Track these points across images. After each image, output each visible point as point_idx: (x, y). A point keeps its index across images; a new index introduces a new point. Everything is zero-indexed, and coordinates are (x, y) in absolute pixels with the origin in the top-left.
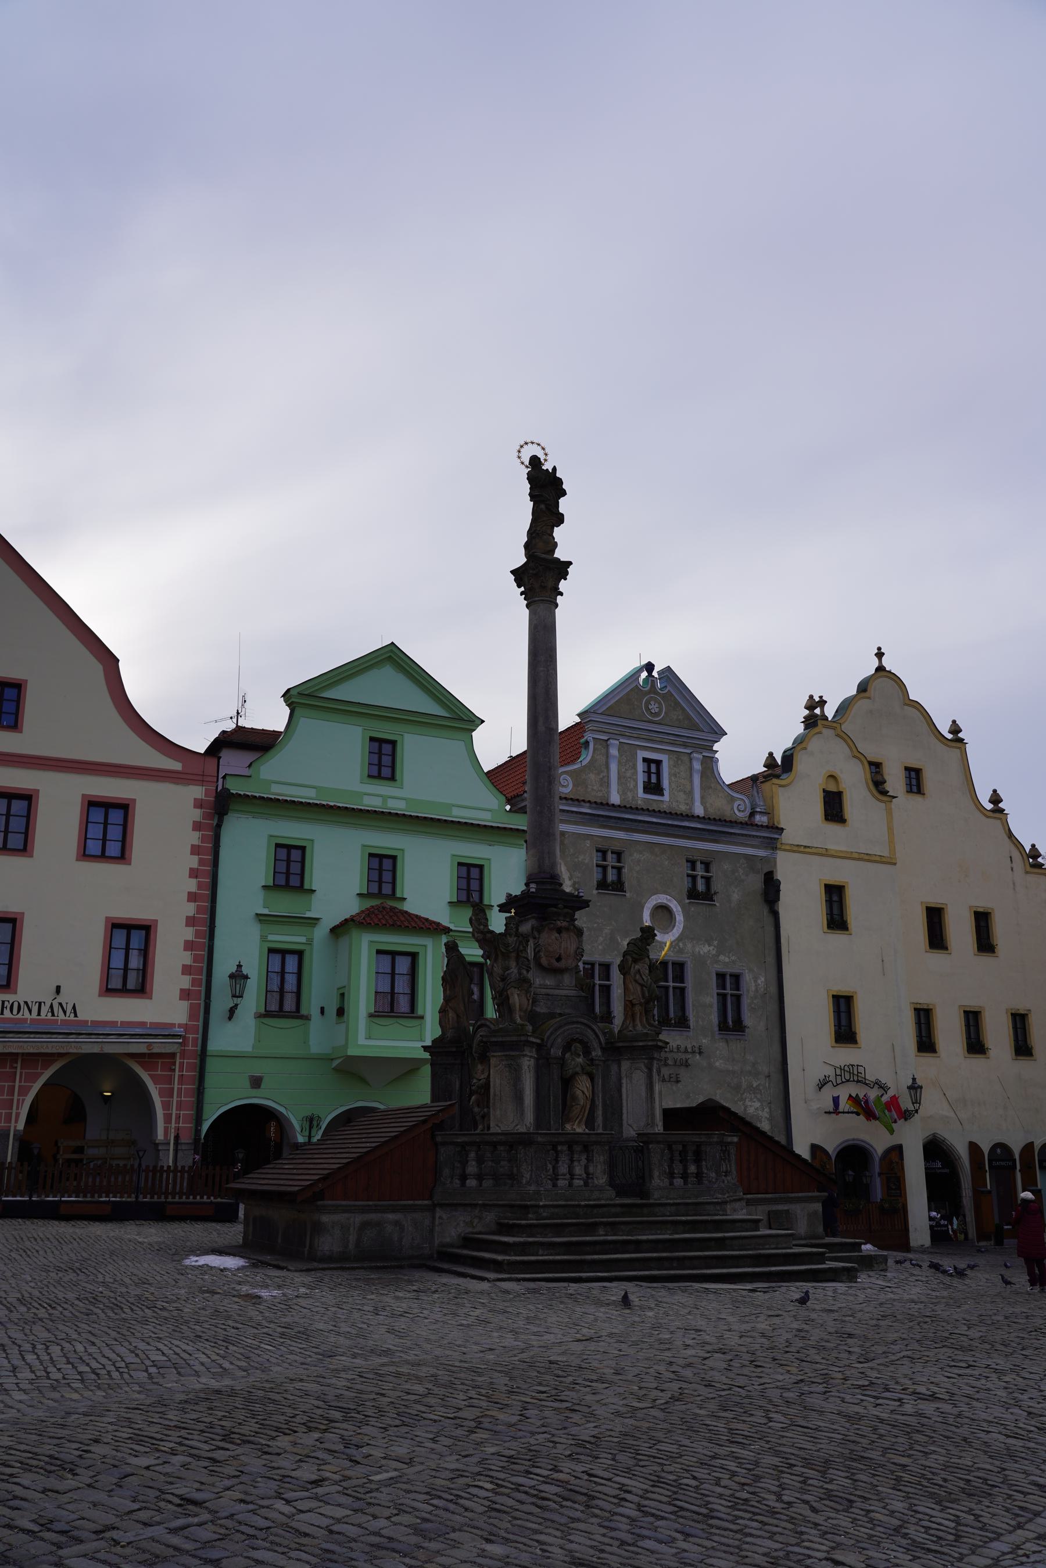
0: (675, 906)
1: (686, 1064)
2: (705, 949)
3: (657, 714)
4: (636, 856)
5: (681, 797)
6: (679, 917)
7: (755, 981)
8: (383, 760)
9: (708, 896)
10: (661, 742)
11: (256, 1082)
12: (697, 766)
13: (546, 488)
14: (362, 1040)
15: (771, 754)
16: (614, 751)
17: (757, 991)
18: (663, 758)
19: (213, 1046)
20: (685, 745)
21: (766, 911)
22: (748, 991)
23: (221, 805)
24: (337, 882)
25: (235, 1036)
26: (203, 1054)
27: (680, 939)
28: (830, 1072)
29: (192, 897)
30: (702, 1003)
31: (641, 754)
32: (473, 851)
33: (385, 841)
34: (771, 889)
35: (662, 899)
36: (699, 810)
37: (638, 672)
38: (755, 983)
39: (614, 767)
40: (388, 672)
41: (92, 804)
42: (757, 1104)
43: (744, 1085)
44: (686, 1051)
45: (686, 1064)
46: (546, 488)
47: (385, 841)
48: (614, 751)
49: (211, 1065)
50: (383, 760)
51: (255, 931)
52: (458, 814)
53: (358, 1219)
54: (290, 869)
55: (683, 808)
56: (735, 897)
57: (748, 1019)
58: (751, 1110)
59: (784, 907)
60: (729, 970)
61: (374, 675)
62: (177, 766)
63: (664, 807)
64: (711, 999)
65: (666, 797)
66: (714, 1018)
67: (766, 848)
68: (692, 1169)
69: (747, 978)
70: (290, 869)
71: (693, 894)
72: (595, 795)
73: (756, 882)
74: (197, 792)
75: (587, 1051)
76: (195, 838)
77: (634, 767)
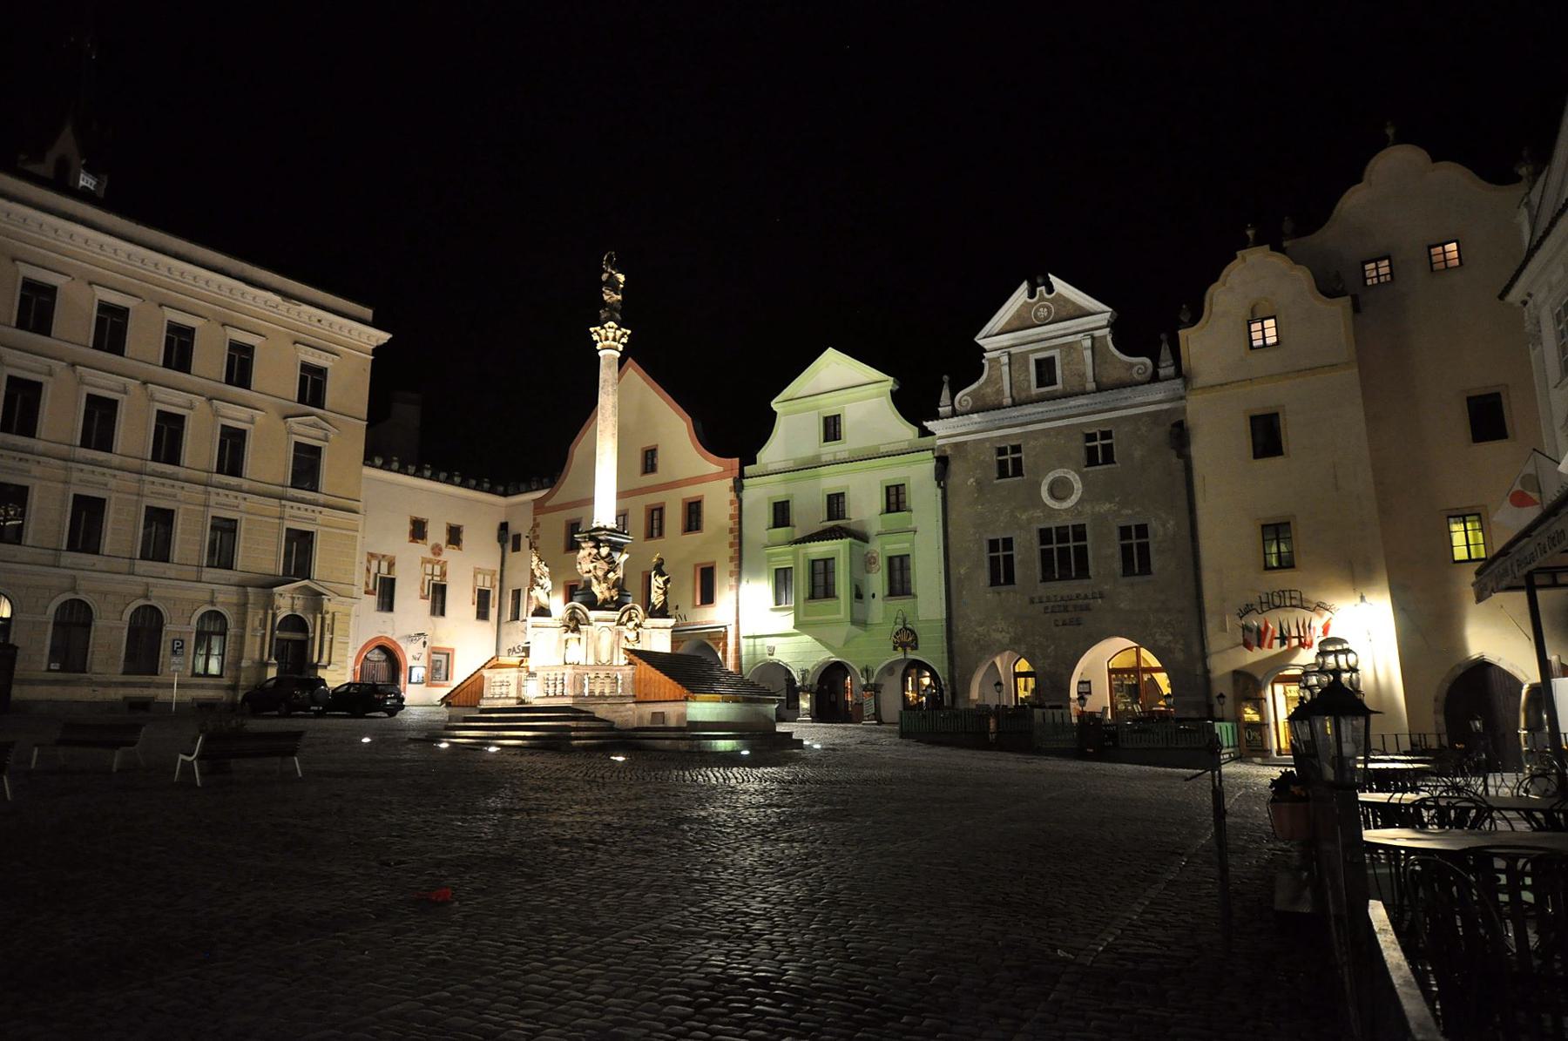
1: (1087, 608)
2: (1107, 506)
6: (1078, 486)
9: (1108, 457)
18: (1056, 353)
27: (1081, 501)
28: (1253, 598)
30: (1104, 553)
31: (1032, 358)
34: (1179, 435)
35: (1059, 473)
38: (1162, 528)
45: (1087, 608)
52: (883, 449)
56: (1138, 453)
57: (1156, 562)
58: (1162, 644)
59: (1200, 451)
60: (1133, 523)
64: (1114, 549)
65: (1059, 386)
66: (1117, 565)
69: (1154, 526)
71: (1092, 459)
74: (729, 482)
77: (1027, 370)
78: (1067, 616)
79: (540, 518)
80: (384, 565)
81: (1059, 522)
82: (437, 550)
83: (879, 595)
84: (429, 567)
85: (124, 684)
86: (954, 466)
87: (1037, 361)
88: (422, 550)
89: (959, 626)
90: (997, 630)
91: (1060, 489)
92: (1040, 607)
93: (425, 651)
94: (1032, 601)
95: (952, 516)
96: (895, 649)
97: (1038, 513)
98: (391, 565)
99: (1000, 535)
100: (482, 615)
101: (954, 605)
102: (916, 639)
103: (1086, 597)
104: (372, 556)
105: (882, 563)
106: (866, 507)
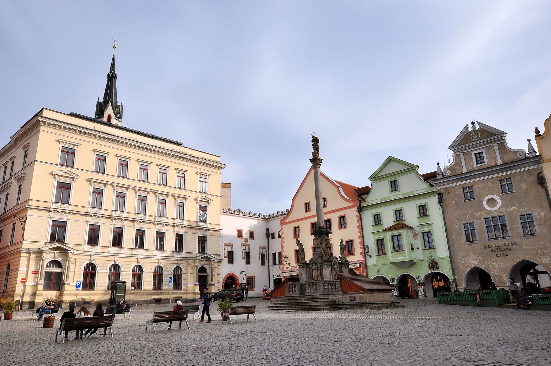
0: (496, 197)
2: (513, 208)
3: (477, 138)
4: (477, 186)
5: (493, 160)
7: (539, 214)
8: (394, 186)
10: (480, 146)
11: (378, 271)
12: (496, 148)
13: (315, 141)
14: (391, 259)
15: (537, 128)
16: (462, 156)
17: (540, 218)
18: (483, 150)
19: (368, 264)
20: (491, 143)
21: (540, 187)
22: (536, 219)
23: (360, 210)
24: (389, 220)
25: (372, 261)
26: (366, 266)
27: (500, 208)
29: (359, 232)
30: (515, 228)
31: (473, 153)
32: (421, 202)
33: (397, 206)
36: (500, 162)
37: (467, 126)
39: (463, 162)
40: (392, 163)
41: (340, 218)
42: (549, 259)
43: (540, 253)
44: (509, 245)
46: (315, 141)
47: (397, 206)
48: (462, 156)
49: (369, 268)
50: (394, 186)
51: (372, 236)
52: (416, 193)
53: (276, 300)
54: (377, 220)
55: (494, 164)
56: (524, 186)
57: (537, 229)
58: (546, 262)
61: (389, 165)
62: (351, 204)
63: (486, 166)
67: (536, 164)
68: (315, 288)
69: (535, 214)
70: (377, 220)
72: (458, 171)
73: (534, 178)
74: (356, 209)
75: (316, 264)
76: (357, 219)
77: (472, 158)
78: (501, 253)
79: (283, 226)
80: (230, 247)
81: (493, 215)
82: (246, 240)
83: (420, 249)
84: (244, 247)
85: (172, 293)
86: (444, 197)
87: (475, 154)
88: (242, 241)
89: (455, 258)
90: (471, 260)
91: (492, 202)
92: (489, 250)
93: (245, 278)
94: (485, 248)
95: (447, 216)
96: (430, 269)
97: (483, 213)
98: (232, 246)
99: (468, 222)
100: (263, 263)
101: (452, 249)
102: (437, 264)
103: (509, 245)
104: (226, 244)
105: (420, 235)
106: (411, 215)
